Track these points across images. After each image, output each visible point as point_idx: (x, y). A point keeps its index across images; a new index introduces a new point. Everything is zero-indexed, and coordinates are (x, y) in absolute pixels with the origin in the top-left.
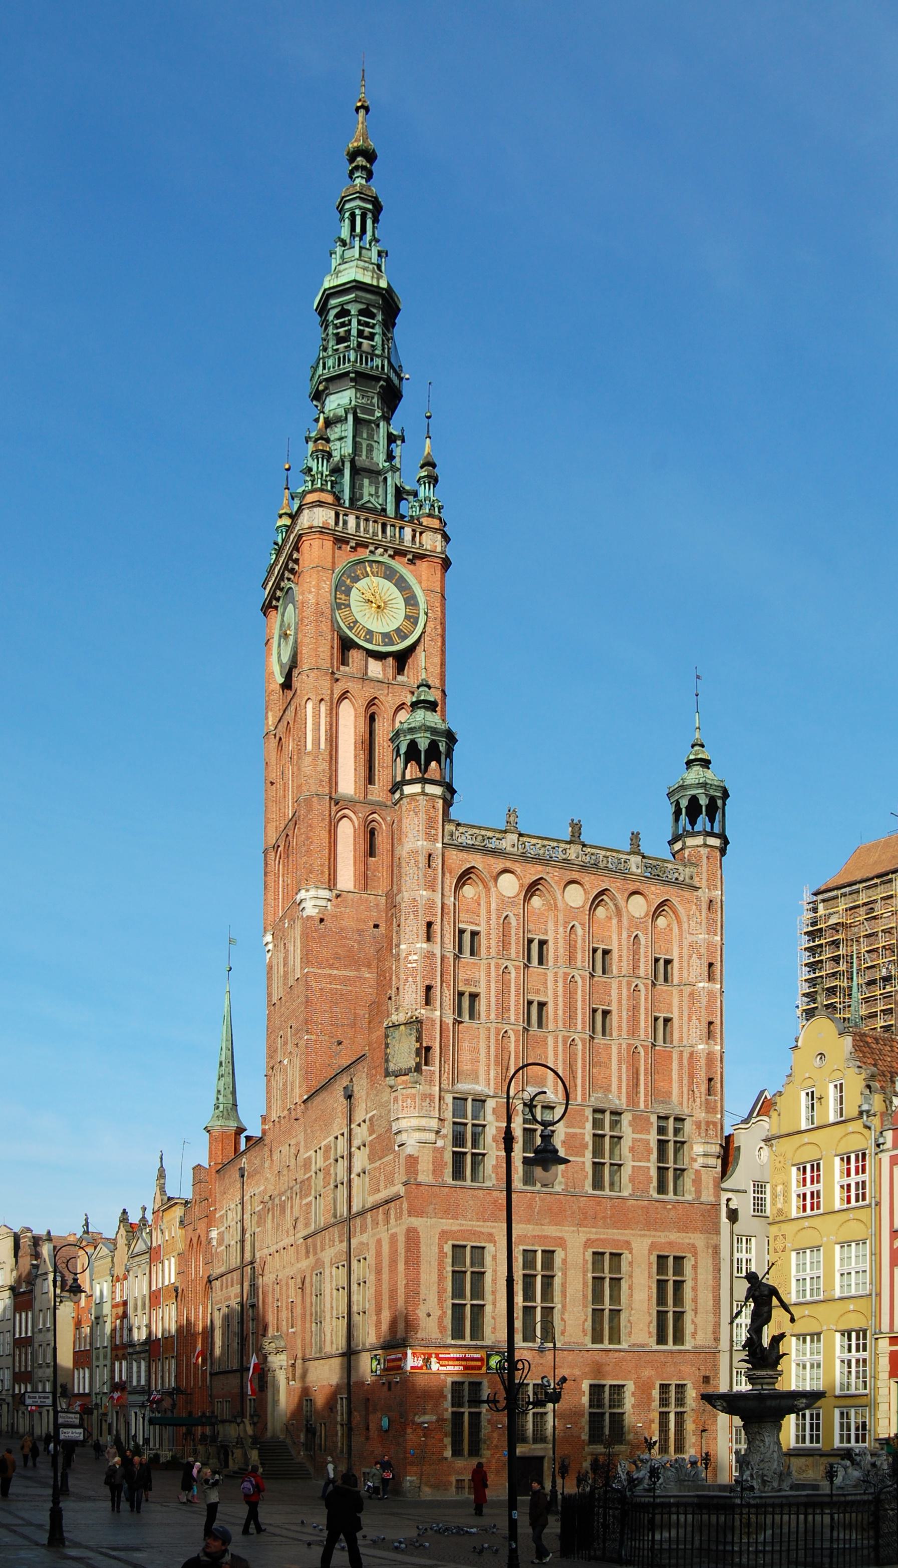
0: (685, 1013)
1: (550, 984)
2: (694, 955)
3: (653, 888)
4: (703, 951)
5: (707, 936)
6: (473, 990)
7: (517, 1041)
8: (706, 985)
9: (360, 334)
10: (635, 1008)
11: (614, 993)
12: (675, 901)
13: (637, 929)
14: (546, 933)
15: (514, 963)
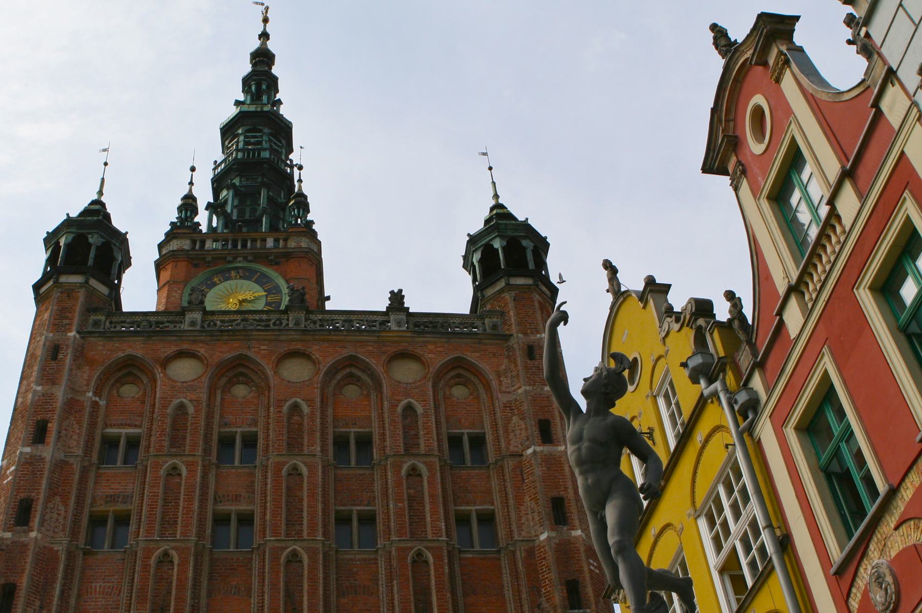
0: (510, 496)
1: (258, 487)
2: (515, 419)
3: (431, 347)
4: (525, 407)
5: (528, 388)
6: (120, 507)
7: (183, 563)
8: (539, 449)
9: (246, 143)
10: (415, 501)
11: (378, 486)
12: (472, 357)
13: (407, 395)
14: (255, 423)
15: (184, 459)
